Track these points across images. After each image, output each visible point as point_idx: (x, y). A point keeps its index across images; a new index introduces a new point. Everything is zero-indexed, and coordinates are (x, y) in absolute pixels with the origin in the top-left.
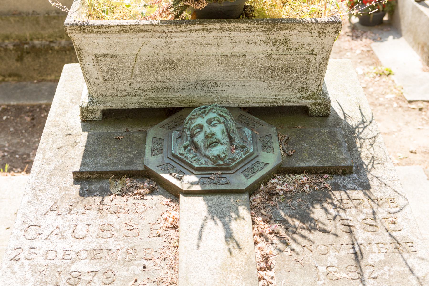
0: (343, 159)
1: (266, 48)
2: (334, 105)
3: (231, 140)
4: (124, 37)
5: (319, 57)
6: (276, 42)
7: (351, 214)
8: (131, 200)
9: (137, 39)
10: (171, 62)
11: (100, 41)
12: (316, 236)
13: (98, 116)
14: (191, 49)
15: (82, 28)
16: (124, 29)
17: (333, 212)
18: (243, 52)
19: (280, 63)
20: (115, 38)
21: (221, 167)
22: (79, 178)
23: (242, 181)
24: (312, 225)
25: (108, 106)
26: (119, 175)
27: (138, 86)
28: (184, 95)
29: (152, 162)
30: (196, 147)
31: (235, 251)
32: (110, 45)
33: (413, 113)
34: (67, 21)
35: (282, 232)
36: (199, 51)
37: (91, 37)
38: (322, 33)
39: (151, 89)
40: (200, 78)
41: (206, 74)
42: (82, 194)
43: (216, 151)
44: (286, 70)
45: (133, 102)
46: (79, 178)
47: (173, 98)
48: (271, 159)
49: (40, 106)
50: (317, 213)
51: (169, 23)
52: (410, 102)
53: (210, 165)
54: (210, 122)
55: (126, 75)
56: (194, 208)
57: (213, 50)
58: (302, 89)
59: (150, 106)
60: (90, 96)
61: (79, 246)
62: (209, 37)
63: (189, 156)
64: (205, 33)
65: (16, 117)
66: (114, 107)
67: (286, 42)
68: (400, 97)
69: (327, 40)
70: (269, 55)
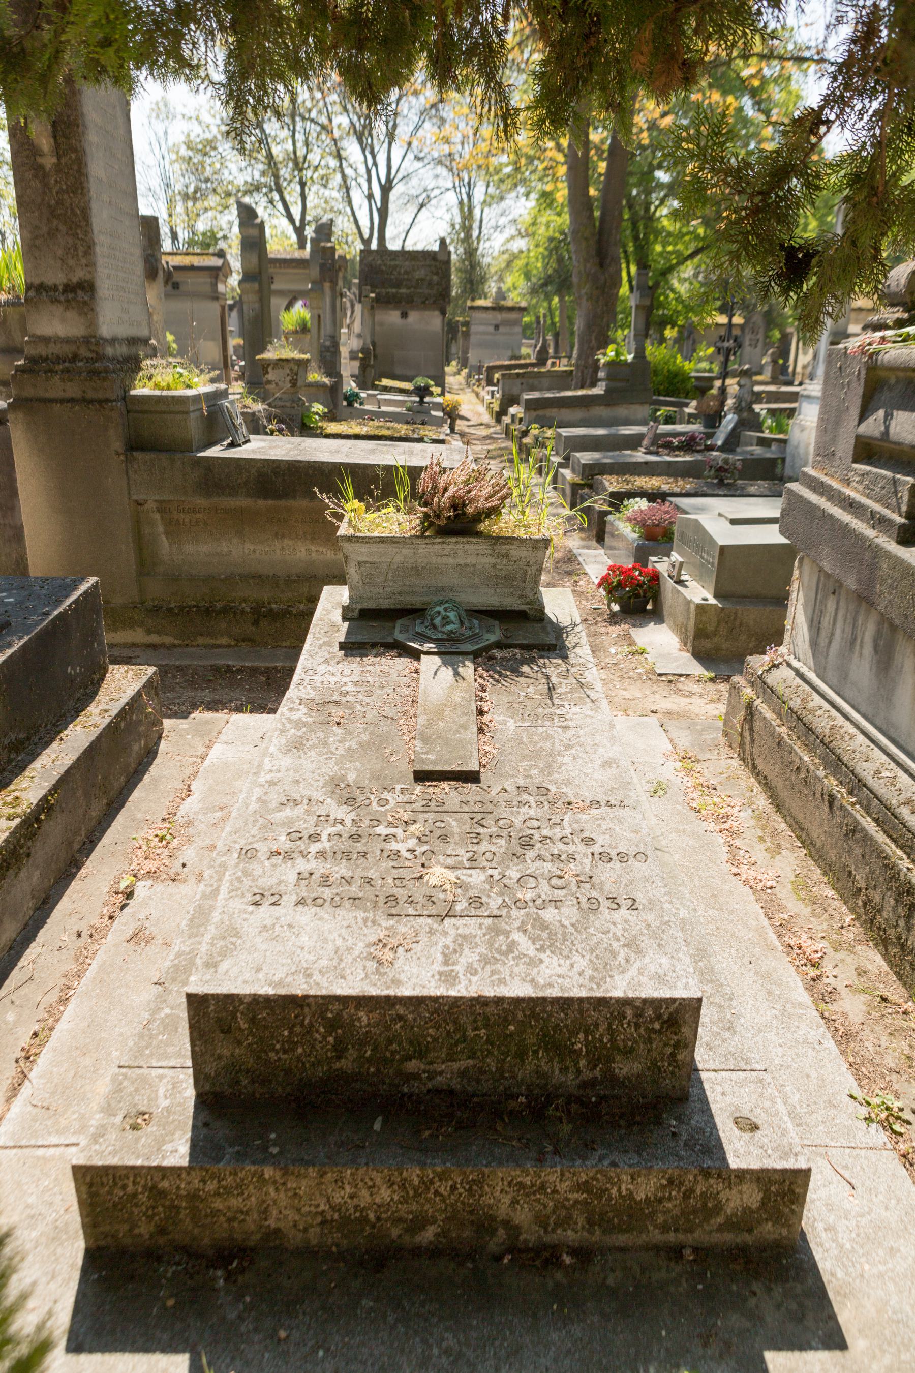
0: (550, 640)
1: (492, 560)
2: (547, 611)
3: (462, 623)
4: (382, 548)
5: (534, 568)
6: (499, 555)
7: (550, 671)
8: (384, 660)
9: (391, 549)
10: (417, 569)
11: (363, 550)
12: (522, 680)
13: (356, 614)
14: (434, 559)
15: (350, 539)
16: (382, 540)
17: (536, 668)
18: (474, 562)
19: (503, 573)
20: (375, 548)
21: (453, 638)
22: (343, 646)
23: (469, 647)
24: (521, 674)
25: (365, 605)
26: (374, 645)
27: (389, 590)
28: (426, 599)
29: (399, 636)
30: (434, 627)
31: (461, 681)
32: (370, 554)
33: (662, 684)
34: (338, 534)
35: (496, 677)
36: (439, 560)
37: (357, 546)
38: (535, 548)
39: (400, 593)
40: (440, 584)
41: (444, 581)
42: (346, 655)
43: (449, 627)
44: (508, 579)
45: (385, 604)
46: (343, 646)
47: (415, 601)
48: (492, 638)
49: (275, 668)
50: (525, 669)
51: (417, 537)
52: (660, 675)
53: (445, 637)
54: (446, 610)
55: (380, 580)
56: (430, 663)
57: (451, 561)
58: (521, 597)
59: (399, 607)
60: (351, 598)
61: (346, 679)
62: (448, 548)
63: (429, 633)
64: (445, 546)
65: (250, 676)
66: (370, 607)
67: (507, 555)
68: (652, 671)
69: (539, 554)
70: (494, 566)
